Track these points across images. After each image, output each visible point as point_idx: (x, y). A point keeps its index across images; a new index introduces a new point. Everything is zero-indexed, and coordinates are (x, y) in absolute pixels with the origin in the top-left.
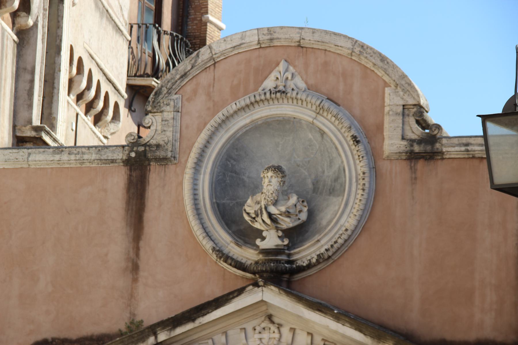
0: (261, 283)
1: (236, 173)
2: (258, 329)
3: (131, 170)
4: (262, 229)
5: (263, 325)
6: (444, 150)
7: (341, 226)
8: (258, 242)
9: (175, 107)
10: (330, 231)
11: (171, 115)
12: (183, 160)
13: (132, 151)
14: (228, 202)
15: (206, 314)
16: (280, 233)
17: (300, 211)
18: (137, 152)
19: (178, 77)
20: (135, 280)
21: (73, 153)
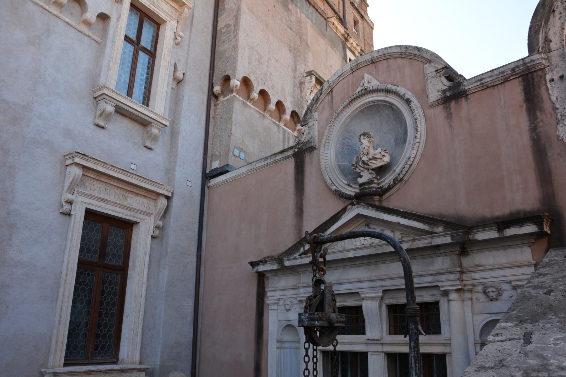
1: (350, 146)
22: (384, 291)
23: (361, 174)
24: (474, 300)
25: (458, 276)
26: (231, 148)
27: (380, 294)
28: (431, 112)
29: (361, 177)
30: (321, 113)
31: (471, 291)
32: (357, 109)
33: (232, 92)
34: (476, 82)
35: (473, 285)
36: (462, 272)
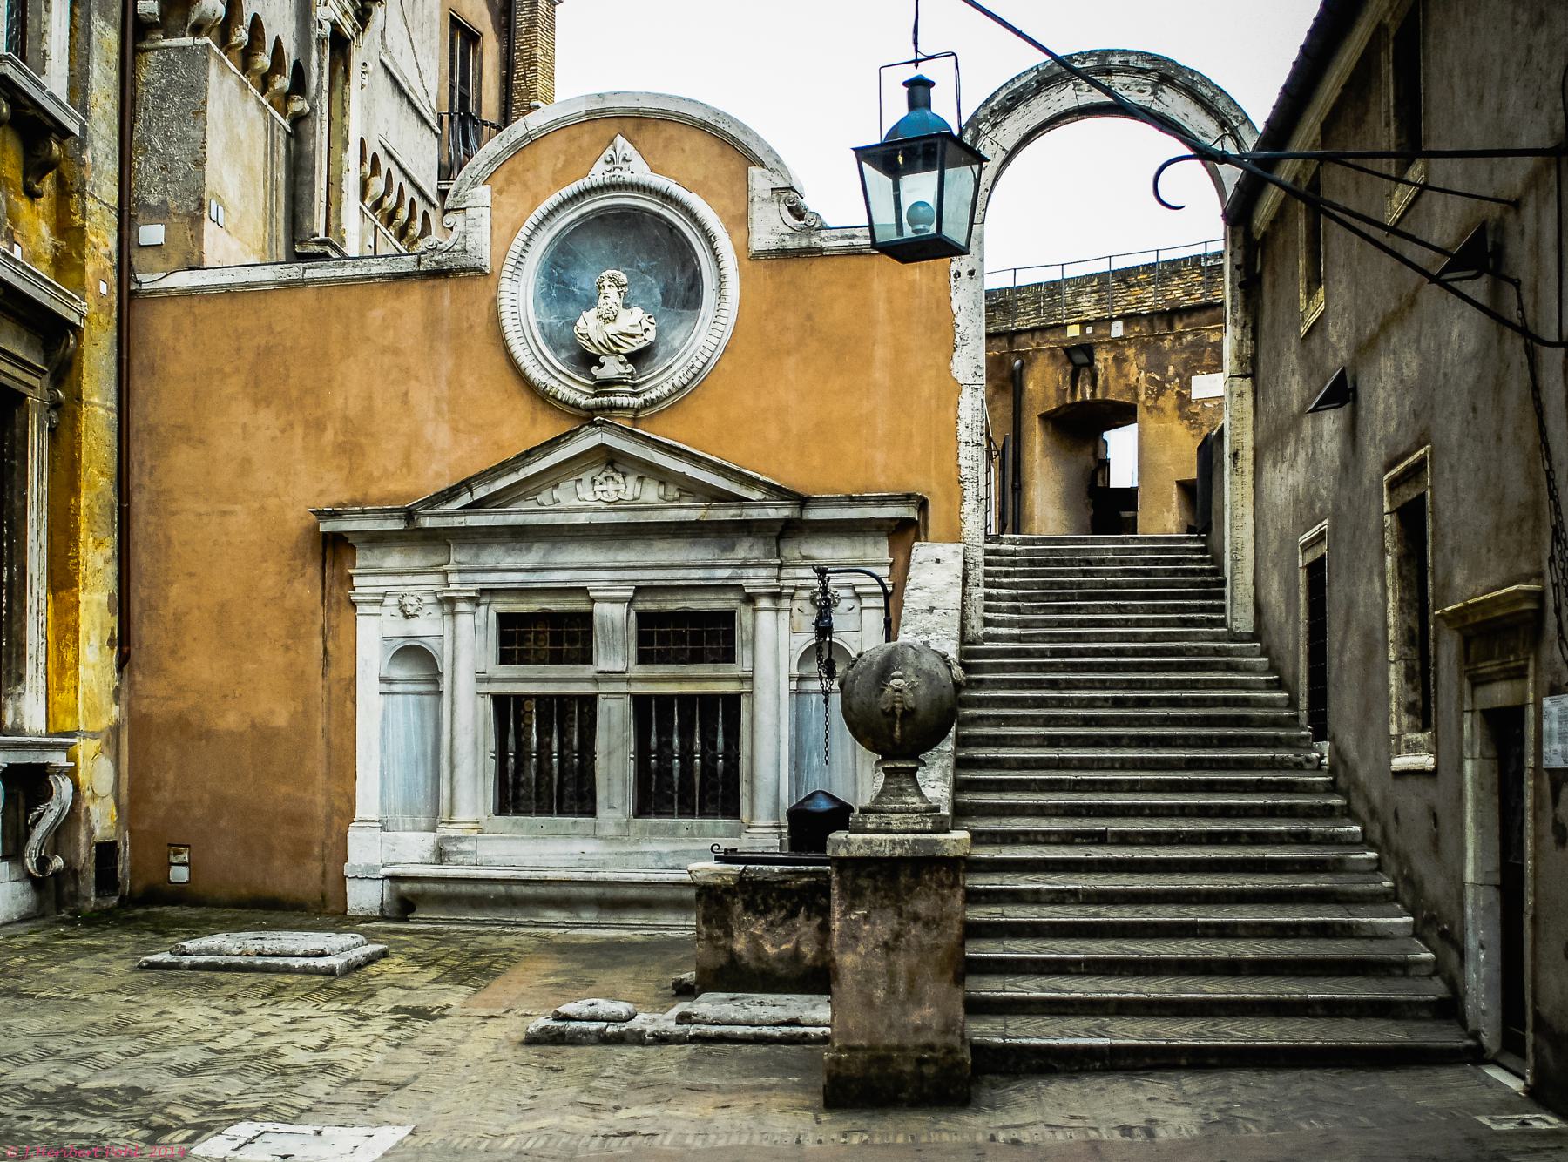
22: (638, 590)
23: (602, 360)
24: (795, 611)
26: (206, 197)
27: (631, 594)
30: (500, 192)
31: (792, 597)
33: (197, 30)
34: (844, 238)
35: (796, 588)
36: (780, 567)
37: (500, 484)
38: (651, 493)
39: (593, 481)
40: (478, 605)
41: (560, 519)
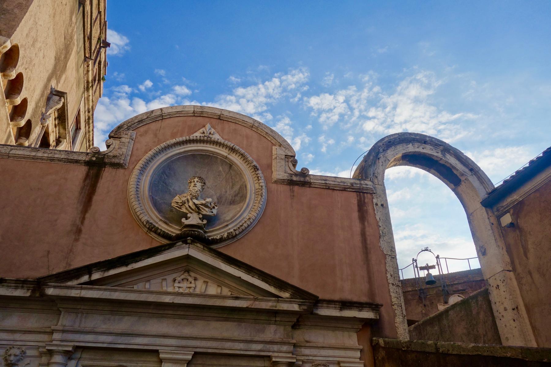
0: (189, 241)
2: (179, 279)
3: (89, 169)
4: (187, 212)
5: (183, 277)
6: (312, 181)
7: (244, 218)
8: (183, 220)
9: (131, 136)
10: (236, 220)
11: (127, 140)
12: (131, 168)
13: (93, 157)
14: (159, 199)
15: (138, 261)
16: (201, 216)
17: (214, 207)
18: (97, 158)
19: (136, 121)
20: (77, 240)
21: (47, 153)
22: (196, 354)
23: (189, 215)
25: (291, 348)
28: (274, 186)
29: (187, 219)
32: (191, 151)
34: (321, 180)
37: (112, 272)
38: (213, 290)
39: (174, 280)
40: (70, 359)
41: (151, 298)
